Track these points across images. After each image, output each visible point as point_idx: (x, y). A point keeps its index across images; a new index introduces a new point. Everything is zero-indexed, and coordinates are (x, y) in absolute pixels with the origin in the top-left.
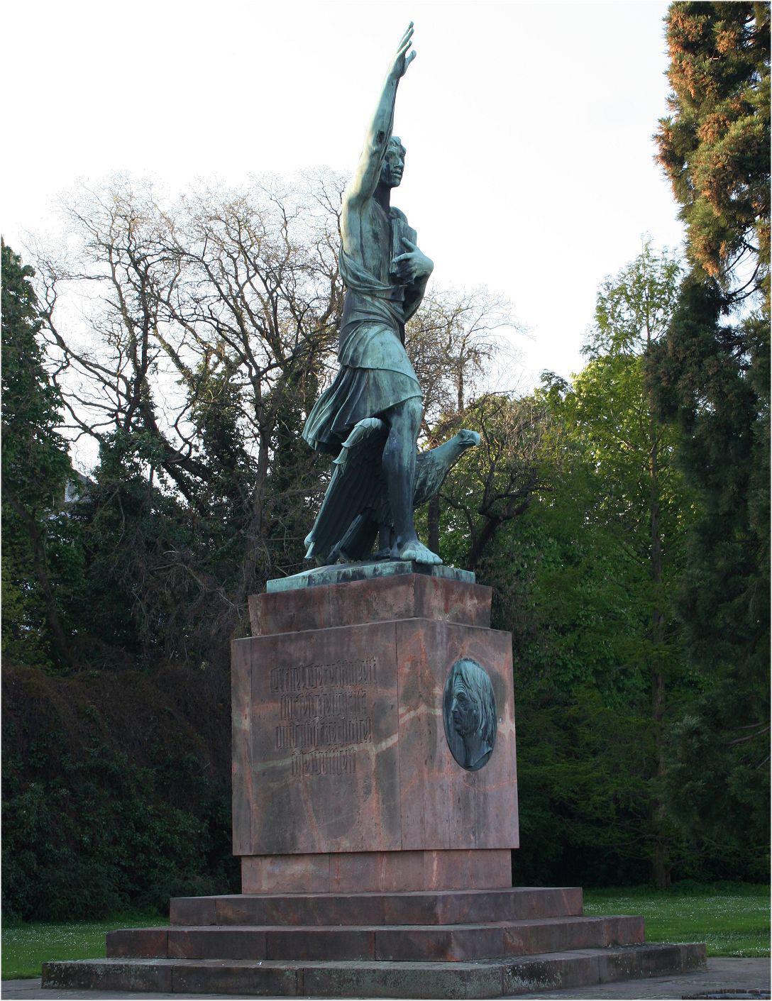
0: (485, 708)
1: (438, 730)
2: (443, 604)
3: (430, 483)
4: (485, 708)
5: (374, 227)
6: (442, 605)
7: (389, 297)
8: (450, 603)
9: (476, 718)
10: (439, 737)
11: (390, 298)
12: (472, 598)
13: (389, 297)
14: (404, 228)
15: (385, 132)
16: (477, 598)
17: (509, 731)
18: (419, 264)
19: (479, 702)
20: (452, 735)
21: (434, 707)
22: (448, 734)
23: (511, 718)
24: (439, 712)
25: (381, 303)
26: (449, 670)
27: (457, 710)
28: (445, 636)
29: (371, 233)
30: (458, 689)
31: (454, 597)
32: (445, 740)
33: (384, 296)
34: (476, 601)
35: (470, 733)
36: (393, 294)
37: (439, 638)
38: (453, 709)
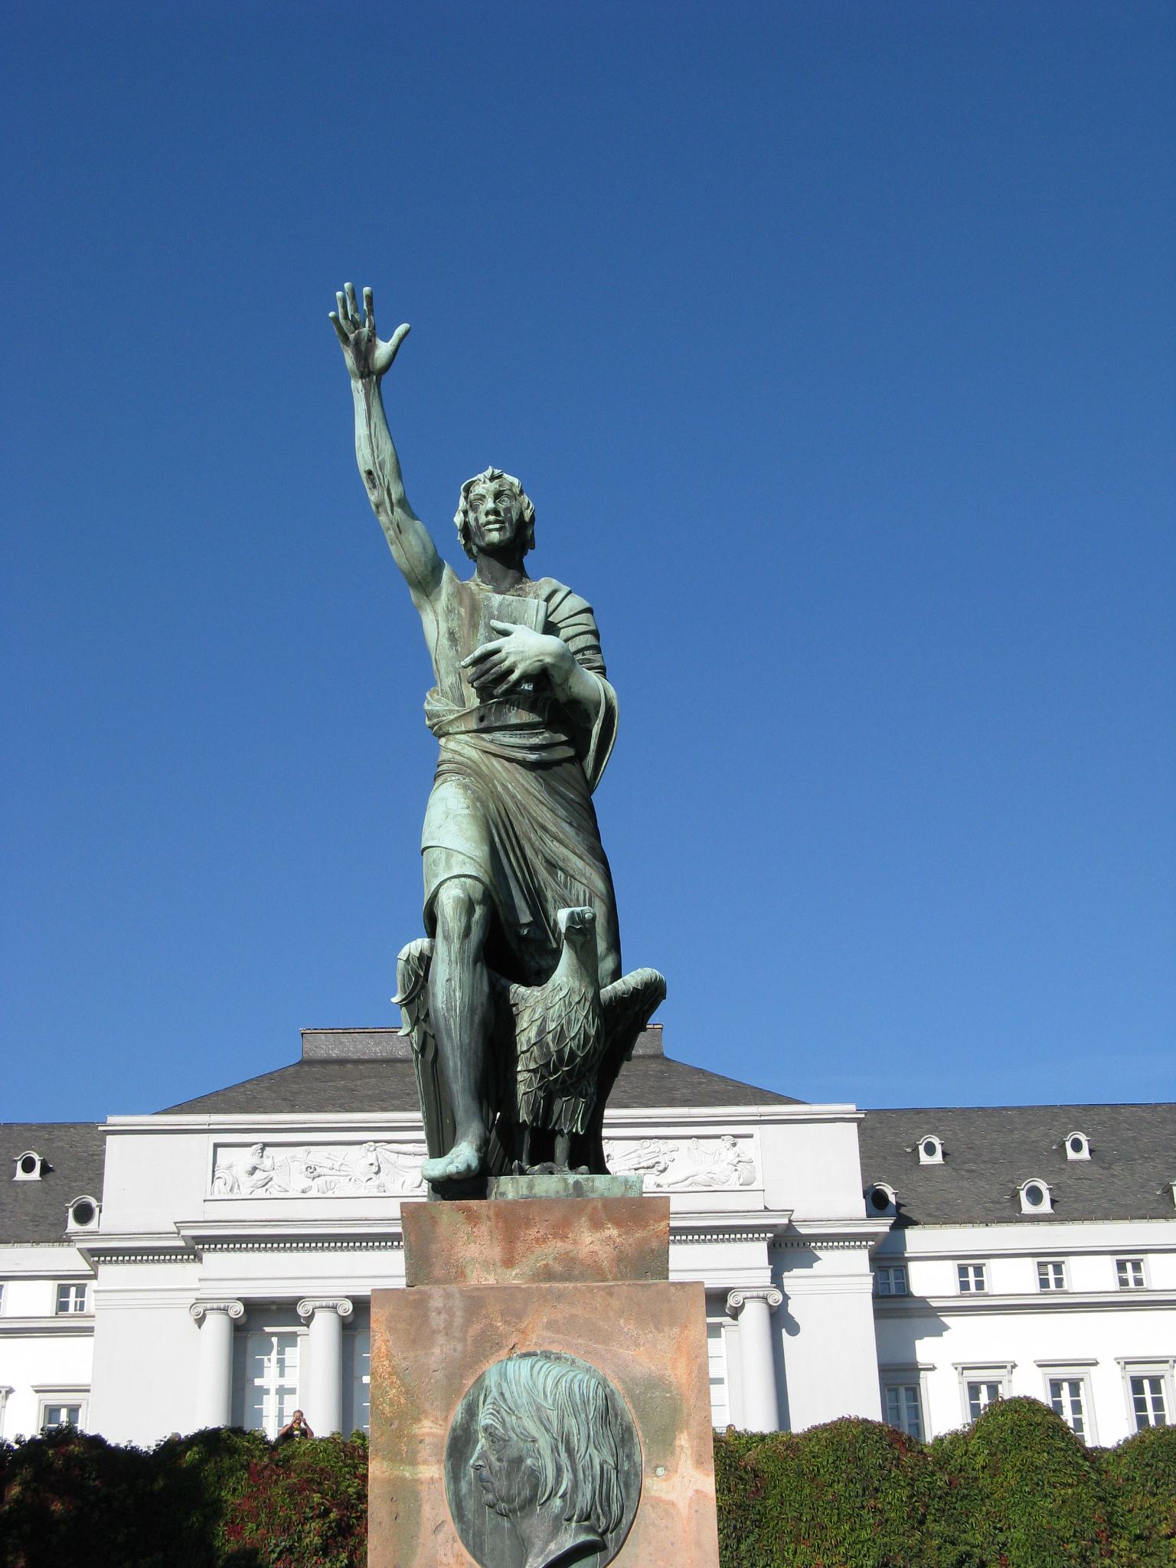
0: (570, 1451)
1: (427, 1510)
2: (498, 1249)
3: (552, 1026)
4: (570, 1451)
5: (449, 625)
6: (496, 1252)
7: (473, 724)
8: (520, 1247)
9: (535, 1477)
10: (427, 1526)
11: (475, 727)
12: (596, 1225)
13: (473, 724)
14: (501, 605)
15: (373, 470)
16: (618, 1224)
17: (690, 1493)
18: (515, 653)
19: (544, 1443)
20: (469, 1515)
21: (413, 1462)
22: (459, 1514)
23: (699, 1462)
24: (432, 1471)
25: (459, 742)
26: (469, 1382)
27: (480, 1463)
28: (459, 1313)
29: (447, 635)
30: (484, 1418)
31: (533, 1233)
32: (451, 1528)
33: (463, 729)
34: (613, 1232)
35: (522, 1508)
36: (482, 719)
37: (437, 1321)
38: (471, 1462)
